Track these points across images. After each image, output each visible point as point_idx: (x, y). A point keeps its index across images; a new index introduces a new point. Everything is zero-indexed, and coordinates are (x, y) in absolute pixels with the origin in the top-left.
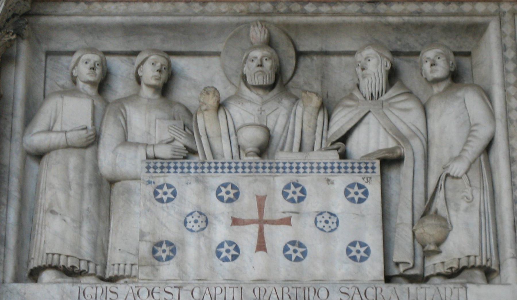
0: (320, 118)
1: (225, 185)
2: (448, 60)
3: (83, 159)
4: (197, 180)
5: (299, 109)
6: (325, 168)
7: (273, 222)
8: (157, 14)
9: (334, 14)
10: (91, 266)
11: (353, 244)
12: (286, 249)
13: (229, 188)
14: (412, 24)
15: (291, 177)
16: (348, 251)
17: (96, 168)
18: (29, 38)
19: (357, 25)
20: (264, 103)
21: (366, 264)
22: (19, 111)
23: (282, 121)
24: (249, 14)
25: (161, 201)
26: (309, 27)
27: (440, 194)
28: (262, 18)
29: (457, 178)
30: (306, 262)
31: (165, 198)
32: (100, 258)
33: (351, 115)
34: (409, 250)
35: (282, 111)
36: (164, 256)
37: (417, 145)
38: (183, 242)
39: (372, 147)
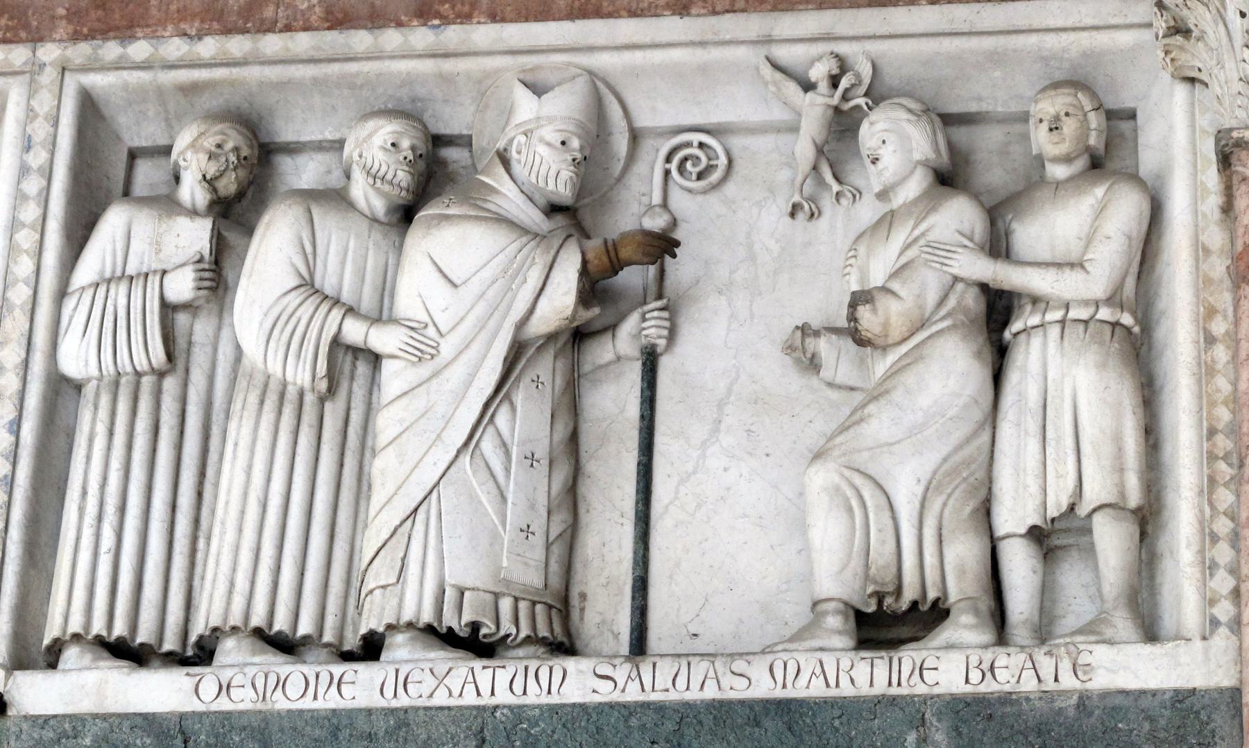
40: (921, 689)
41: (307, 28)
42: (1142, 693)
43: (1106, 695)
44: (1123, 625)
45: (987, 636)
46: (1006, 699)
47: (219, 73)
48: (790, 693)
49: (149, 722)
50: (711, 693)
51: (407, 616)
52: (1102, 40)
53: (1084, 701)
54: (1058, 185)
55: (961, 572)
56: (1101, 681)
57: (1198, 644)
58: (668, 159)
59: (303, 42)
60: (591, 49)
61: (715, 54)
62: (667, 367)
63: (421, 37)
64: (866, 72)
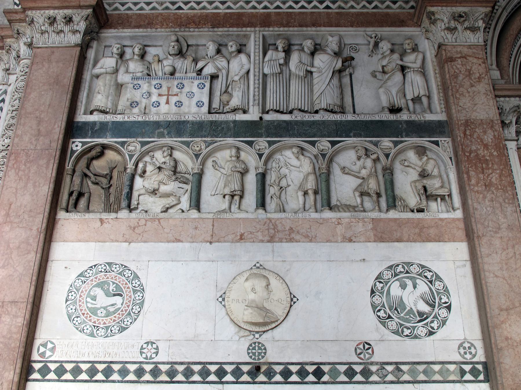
0: (193, 64)
1: (157, 84)
2: (236, 46)
3: (112, 77)
4: (148, 82)
5: (186, 61)
6: (192, 78)
7: (172, 95)
8: (141, 32)
9: (200, 32)
10: (111, 110)
11: (199, 102)
12: (176, 103)
13: (158, 85)
14: (226, 34)
15: (180, 81)
16: (197, 104)
17: (116, 80)
18: (97, 40)
19: (207, 35)
20: (174, 60)
21: (202, 108)
22: (92, 62)
23: (180, 65)
24: (171, 32)
25: (135, 89)
26: (191, 36)
27: (230, 87)
28: (175, 33)
29: (236, 81)
30: (182, 108)
31: (137, 88)
32: (114, 108)
33: (203, 63)
34: (218, 104)
35: (180, 62)
36: (134, 106)
37: (224, 72)
38: (141, 102)
39: (210, 72)
40: (401, 119)
41: (296, 27)
42: (433, 121)
43: (428, 121)
44: (428, 111)
45: (409, 113)
46: (413, 121)
47: (284, 33)
48: (382, 119)
49: (285, 121)
50: (370, 119)
51: (322, 107)
52: (414, 33)
53: (425, 121)
54: (409, 53)
55: (404, 104)
56: (427, 119)
57: (440, 114)
58: (350, 48)
59: (296, 29)
60: (339, 31)
61: (358, 33)
62: (353, 76)
63: (314, 29)
64: (380, 36)
